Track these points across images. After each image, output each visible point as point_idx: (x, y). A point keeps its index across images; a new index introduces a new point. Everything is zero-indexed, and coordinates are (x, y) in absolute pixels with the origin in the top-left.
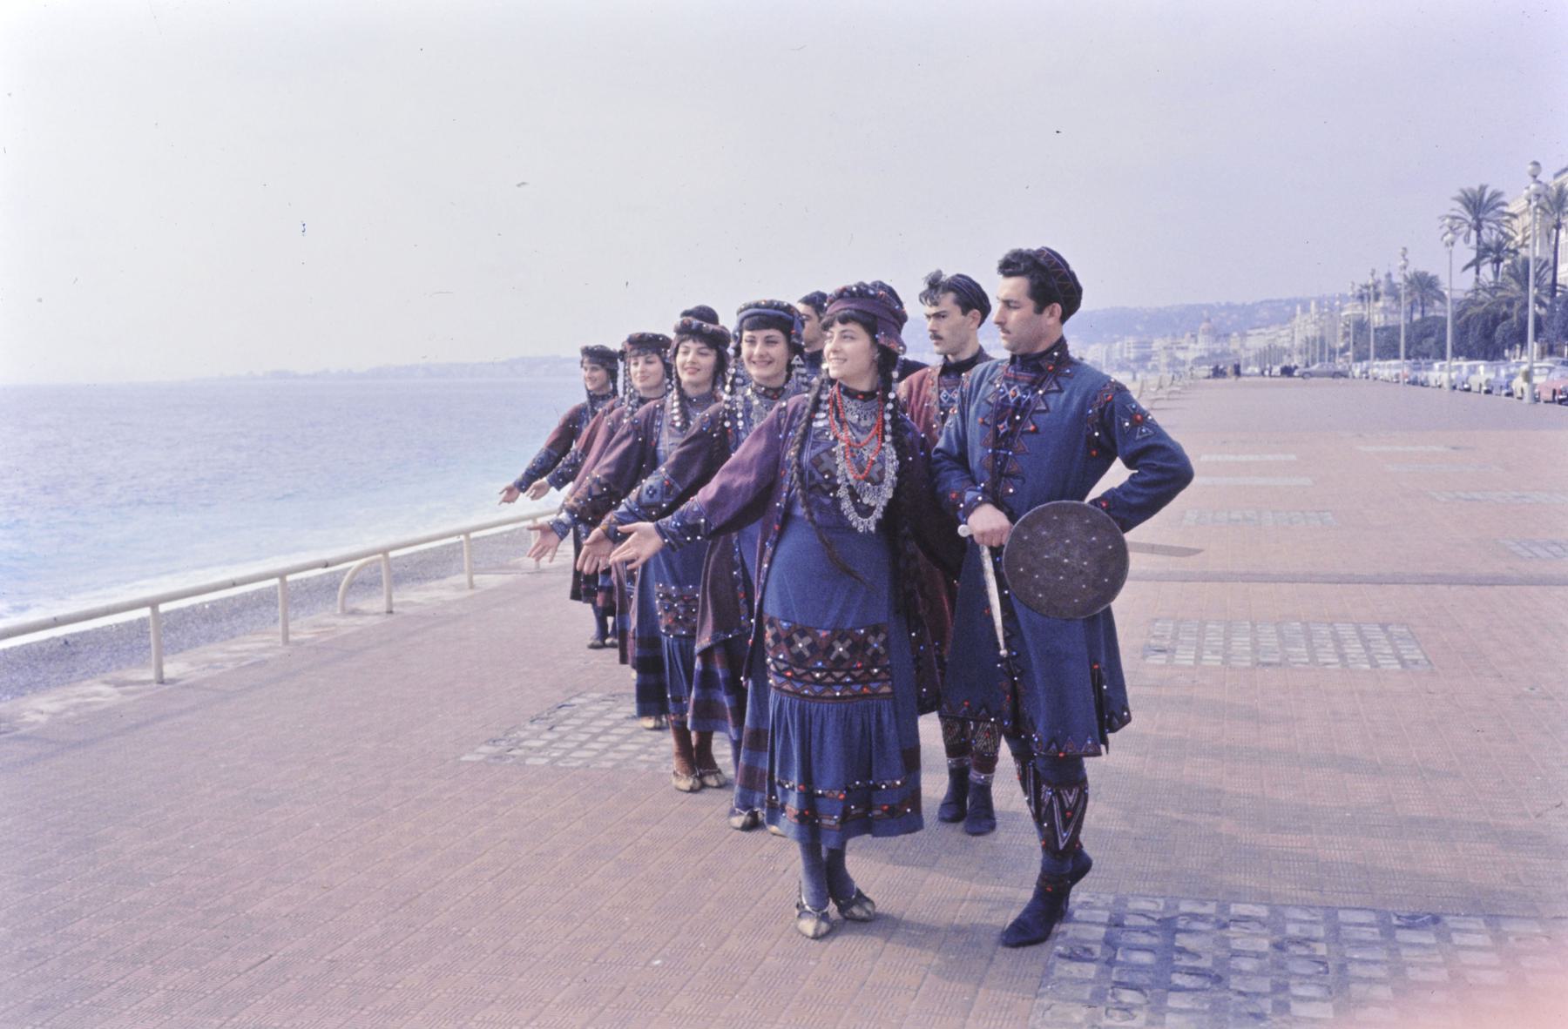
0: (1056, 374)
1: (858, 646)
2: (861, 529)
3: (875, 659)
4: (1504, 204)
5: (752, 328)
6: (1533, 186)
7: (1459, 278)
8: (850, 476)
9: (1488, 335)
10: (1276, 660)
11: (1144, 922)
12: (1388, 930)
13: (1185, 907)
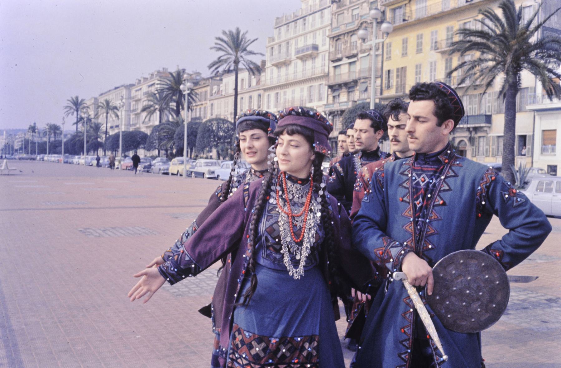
7: (69, 127)
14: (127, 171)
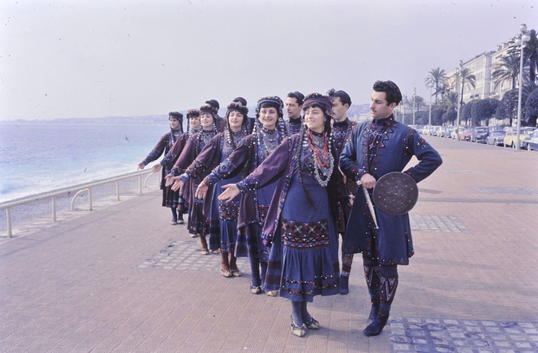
0: (391, 127)
1: (318, 228)
2: (322, 185)
3: (323, 232)
4: (445, 74)
5: (264, 107)
6: (460, 69)
8: (319, 165)
9: (440, 117)
10: (417, 228)
11: (416, 327)
12: (502, 328)
13: (429, 321)
14: (466, 141)
